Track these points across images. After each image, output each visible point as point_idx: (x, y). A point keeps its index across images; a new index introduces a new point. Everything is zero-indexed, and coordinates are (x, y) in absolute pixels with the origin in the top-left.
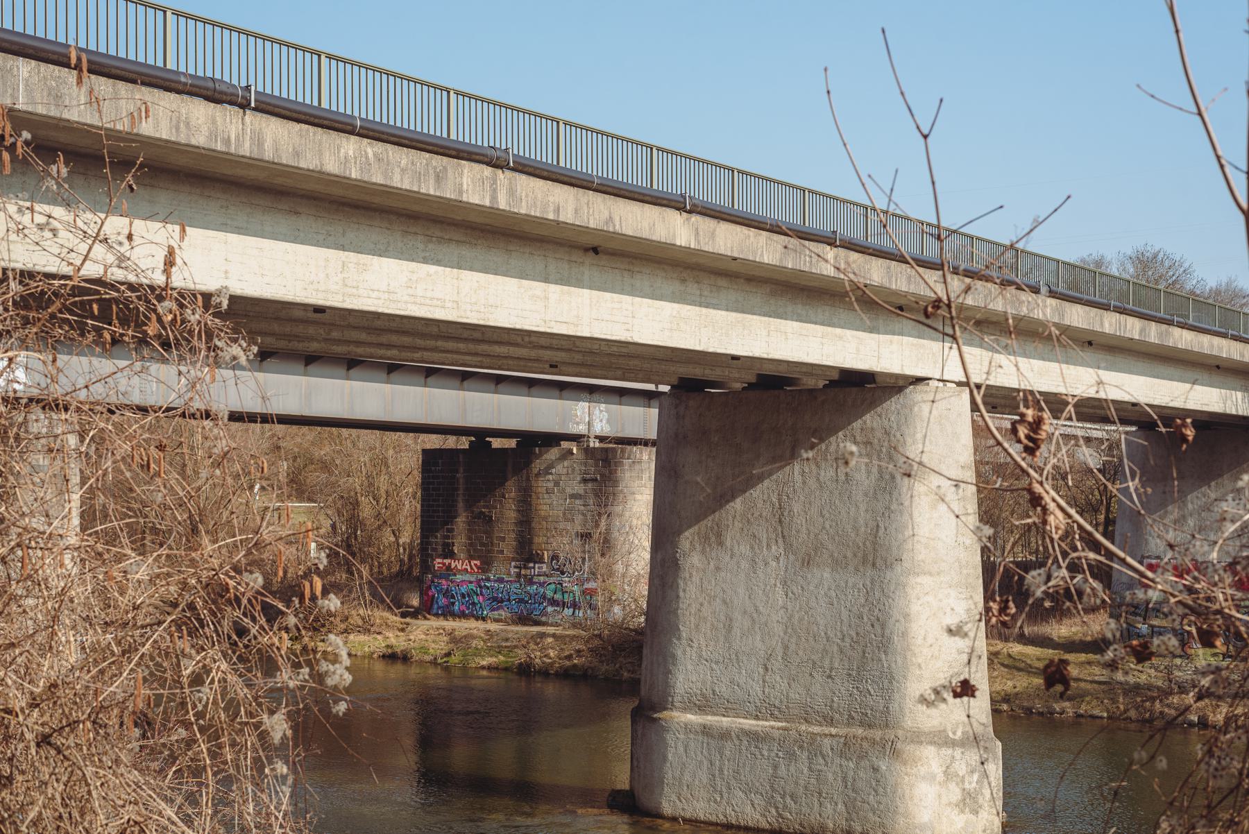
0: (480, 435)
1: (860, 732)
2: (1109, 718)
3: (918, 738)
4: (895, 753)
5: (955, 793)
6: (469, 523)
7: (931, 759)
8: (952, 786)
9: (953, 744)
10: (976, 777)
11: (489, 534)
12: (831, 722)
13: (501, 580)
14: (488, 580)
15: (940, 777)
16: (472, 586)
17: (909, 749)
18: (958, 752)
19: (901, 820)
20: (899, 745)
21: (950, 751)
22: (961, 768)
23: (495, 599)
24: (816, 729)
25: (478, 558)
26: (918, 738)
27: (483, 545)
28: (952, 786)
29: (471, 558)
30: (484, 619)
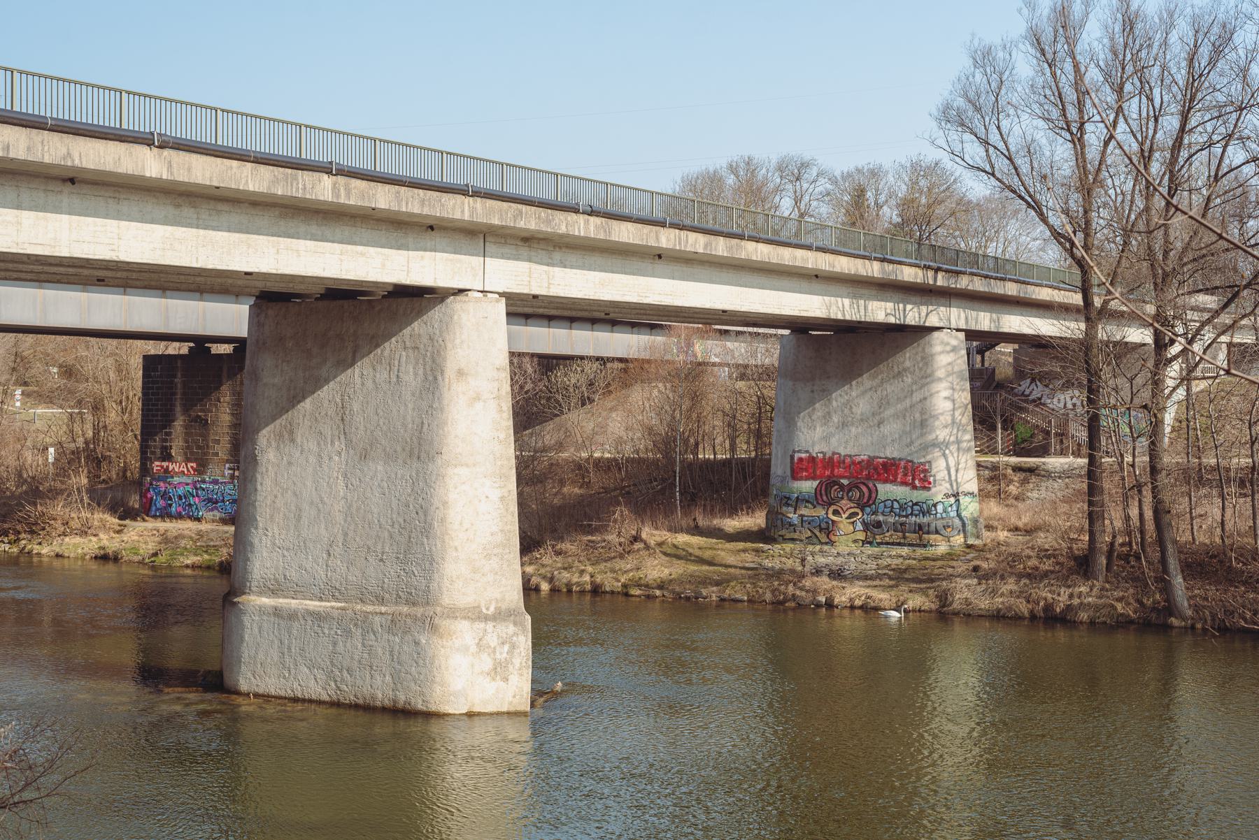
0: (200, 342)
1: (405, 609)
2: (749, 601)
3: (453, 613)
4: (434, 628)
5: (487, 663)
6: (186, 427)
7: (464, 633)
8: (485, 656)
9: (486, 618)
10: (506, 648)
11: (205, 437)
12: (382, 601)
13: (215, 482)
14: (204, 481)
15: (473, 649)
16: (188, 488)
17: (444, 624)
18: (490, 625)
19: (438, 689)
20: (437, 621)
21: (482, 625)
22: (492, 640)
23: (210, 500)
24: (369, 608)
25: (195, 461)
26: (453, 613)
27: (199, 447)
28: (485, 656)
29: (187, 460)
30: (198, 520)
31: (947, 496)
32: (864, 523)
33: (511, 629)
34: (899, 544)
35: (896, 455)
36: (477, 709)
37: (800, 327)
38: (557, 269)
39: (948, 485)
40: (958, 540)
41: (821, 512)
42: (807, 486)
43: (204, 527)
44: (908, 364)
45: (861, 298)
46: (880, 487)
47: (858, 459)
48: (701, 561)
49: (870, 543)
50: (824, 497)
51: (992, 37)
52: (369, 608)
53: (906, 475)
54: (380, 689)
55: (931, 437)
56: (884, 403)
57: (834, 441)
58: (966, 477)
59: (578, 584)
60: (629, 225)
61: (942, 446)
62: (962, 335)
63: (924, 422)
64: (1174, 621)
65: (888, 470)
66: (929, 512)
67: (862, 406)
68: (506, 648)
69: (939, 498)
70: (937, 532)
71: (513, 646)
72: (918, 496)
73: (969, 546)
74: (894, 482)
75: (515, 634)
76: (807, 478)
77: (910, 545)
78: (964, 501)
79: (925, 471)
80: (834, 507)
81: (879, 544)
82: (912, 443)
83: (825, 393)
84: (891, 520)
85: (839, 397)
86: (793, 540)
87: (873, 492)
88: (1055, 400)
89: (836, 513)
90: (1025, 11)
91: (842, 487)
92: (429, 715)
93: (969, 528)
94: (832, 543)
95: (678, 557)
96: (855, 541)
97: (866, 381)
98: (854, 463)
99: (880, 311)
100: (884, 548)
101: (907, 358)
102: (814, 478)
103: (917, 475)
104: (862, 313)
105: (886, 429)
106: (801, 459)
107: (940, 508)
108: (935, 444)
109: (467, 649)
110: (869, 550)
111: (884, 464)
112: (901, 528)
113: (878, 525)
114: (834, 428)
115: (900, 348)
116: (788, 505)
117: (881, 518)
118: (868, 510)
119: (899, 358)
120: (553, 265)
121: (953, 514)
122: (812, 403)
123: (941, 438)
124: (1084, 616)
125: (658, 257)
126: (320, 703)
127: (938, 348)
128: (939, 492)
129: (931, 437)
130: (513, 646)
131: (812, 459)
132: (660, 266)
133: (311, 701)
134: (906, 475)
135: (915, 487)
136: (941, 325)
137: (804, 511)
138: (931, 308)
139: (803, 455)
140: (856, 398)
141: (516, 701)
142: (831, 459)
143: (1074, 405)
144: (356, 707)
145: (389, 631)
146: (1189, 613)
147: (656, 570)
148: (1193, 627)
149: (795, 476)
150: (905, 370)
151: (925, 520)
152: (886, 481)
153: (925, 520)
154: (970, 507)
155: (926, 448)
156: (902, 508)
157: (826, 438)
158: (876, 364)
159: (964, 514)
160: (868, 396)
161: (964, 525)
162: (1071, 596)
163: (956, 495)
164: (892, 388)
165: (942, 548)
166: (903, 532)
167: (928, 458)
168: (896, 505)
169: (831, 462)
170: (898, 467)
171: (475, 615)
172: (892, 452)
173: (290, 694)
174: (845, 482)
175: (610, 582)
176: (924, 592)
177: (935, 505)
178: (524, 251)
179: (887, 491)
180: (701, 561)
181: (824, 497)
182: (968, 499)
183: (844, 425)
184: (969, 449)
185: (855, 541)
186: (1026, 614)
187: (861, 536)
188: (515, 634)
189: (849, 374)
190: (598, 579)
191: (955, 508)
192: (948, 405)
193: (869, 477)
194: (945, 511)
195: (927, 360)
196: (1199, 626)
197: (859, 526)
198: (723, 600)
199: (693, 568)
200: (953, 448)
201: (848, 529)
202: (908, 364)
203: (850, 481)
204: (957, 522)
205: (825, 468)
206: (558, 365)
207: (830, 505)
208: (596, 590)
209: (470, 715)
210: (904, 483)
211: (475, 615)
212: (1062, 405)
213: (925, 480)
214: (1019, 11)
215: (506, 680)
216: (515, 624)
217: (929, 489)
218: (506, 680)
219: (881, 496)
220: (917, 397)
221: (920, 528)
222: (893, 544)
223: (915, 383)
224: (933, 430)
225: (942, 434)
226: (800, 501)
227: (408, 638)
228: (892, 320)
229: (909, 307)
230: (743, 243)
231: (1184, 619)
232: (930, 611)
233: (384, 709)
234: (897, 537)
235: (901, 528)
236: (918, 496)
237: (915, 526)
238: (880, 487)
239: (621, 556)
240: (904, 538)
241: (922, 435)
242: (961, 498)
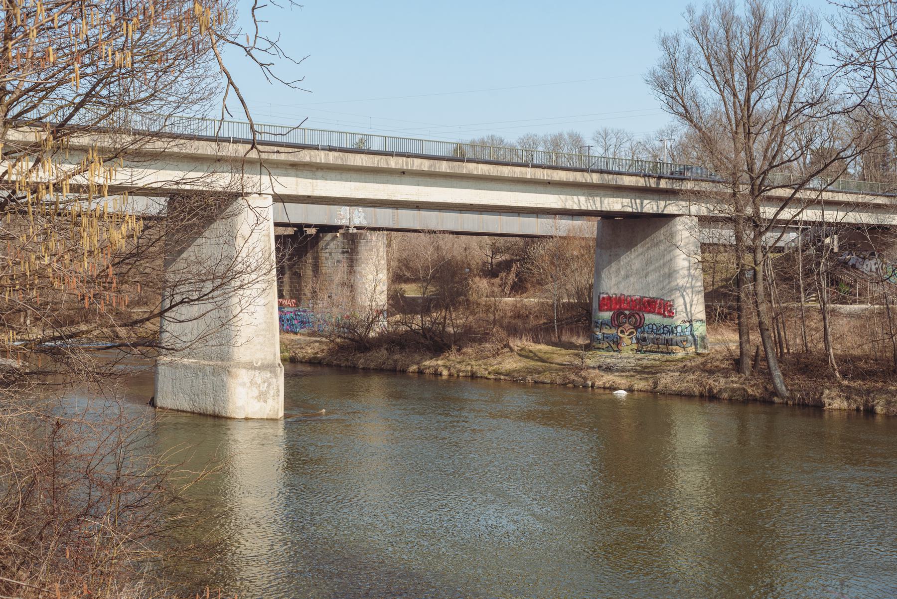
0: (300, 227)
1: (219, 363)
2: (551, 383)
3: (239, 365)
4: (229, 373)
5: (255, 392)
6: (291, 278)
7: (243, 375)
8: (254, 389)
9: (255, 368)
10: (266, 384)
11: (300, 284)
12: (211, 359)
13: (305, 311)
14: (299, 311)
15: (248, 384)
16: (292, 315)
17: (234, 370)
18: (257, 372)
19: (231, 405)
20: (230, 369)
21: (253, 372)
22: (259, 380)
23: (302, 322)
24: (206, 362)
25: (295, 298)
26: (239, 365)
27: (297, 290)
28: (254, 389)
29: (291, 298)
30: (296, 334)
31: (684, 322)
32: (637, 339)
33: (269, 375)
34: (656, 352)
35: (655, 295)
36: (250, 416)
37: (607, 217)
38: (319, 181)
39: (685, 315)
40: (692, 349)
41: (613, 331)
42: (607, 315)
43: (298, 337)
44: (662, 237)
45: (597, 195)
46: (646, 315)
47: (634, 298)
48: (542, 360)
49: (640, 351)
50: (615, 323)
51: (670, 32)
52: (206, 362)
53: (660, 308)
54: (209, 406)
55: (674, 284)
56: (648, 263)
57: (621, 286)
58: (697, 310)
59: (463, 371)
60: (363, 156)
61: (681, 289)
62: (696, 219)
63: (670, 275)
64: (776, 399)
65: (650, 305)
66: (673, 332)
67: (637, 264)
68: (266, 384)
69: (679, 323)
70: (677, 345)
71: (270, 384)
72: (666, 321)
73: (698, 354)
74: (653, 312)
75: (271, 377)
76: (607, 310)
77: (662, 353)
78: (696, 325)
79: (671, 306)
80: (621, 328)
81: (645, 352)
82: (664, 288)
83: (617, 257)
84: (651, 337)
85: (624, 259)
86: (599, 348)
87: (642, 319)
88: (865, 266)
89: (622, 332)
90: (687, 14)
91: (625, 315)
92: (230, 418)
93: (699, 342)
94: (619, 351)
95: (527, 357)
96: (632, 350)
97: (639, 249)
98: (632, 300)
99: (650, 206)
100: (647, 354)
101: (661, 234)
102: (610, 310)
103: (665, 308)
104: (639, 206)
105: (650, 278)
106: (604, 298)
107: (679, 329)
108: (678, 288)
109: (245, 384)
110: (639, 355)
111: (648, 301)
112: (656, 342)
113: (644, 339)
114: (622, 279)
115: (657, 228)
116: (597, 327)
117: (646, 335)
118: (639, 330)
119: (657, 234)
120: (316, 179)
121: (688, 333)
122: (610, 263)
123: (681, 284)
124: (725, 395)
125: (402, 174)
126: (187, 412)
127: (680, 227)
128: (679, 319)
129: (674, 284)
130: (270, 384)
131: (610, 298)
132: (405, 178)
133: (183, 411)
134: (660, 308)
135: (665, 316)
136: (681, 212)
137: (605, 331)
138: (668, 202)
139: (605, 296)
140: (633, 259)
141: (271, 413)
142: (620, 298)
143: (877, 269)
144: (200, 414)
145: (212, 374)
146: (787, 394)
147: (510, 363)
148: (787, 403)
149: (601, 310)
150: (660, 241)
151: (670, 337)
152: (649, 312)
153: (670, 337)
154: (700, 329)
155: (672, 291)
156: (658, 329)
157: (617, 284)
158: (645, 238)
159: (695, 333)
160: (640, 258)
161: (695, 340)
162: (726, 383)
163: (690, 321)
164: (653, 252)
165: (681, 354)
166: (658, 344)
167: (673, 297)
168: (655, 327)
169: (620, 300)
170: (656, 302)
171: (250, 366)
172: (652, 294)
173: (176, 408)
174: (627, 312)
175: (481, 371)
176: (647, 379)
177: (676, 328)
178: (293, 172)
179: (651, 318)
180: (542, 360)
181: (615, 323)
182: (698, 324)
183: (627, 277)
184: (699, 292)
185: (632, 350)
186: (697, 394)
187: (635, 347)
188: (271, 377)
189: (630, 245)
190: (475, 368)
191: (689, 329)
192: (686, 264)
193: (640, 310)
194: (682, 331)
195: (672, 235)
196: (790, 402)
197: (634, 341)
198: (536, 382)
199: (532, 364)
200: (689, 291)
201: (628, 342)
202: (662, 237)
203: (631, 311)
204: (690, 338)
205: (616, 304)
206: (533, 242)
207: (619, 327)
208: (473, 376)
209: (246, 419)
210: (659, 314)
211: (250, 366)
212: (868, 269)
213: (670, 311)
214: (683, 15)
215: (265, 401)
216: (271, 372)
217: (672, 317)
218: (265, 401)
219: (647, 322)
220: (667, 258)
221: (667, 342)
222: (652, 352)
223: (665, 250)
224: (676, 279)
225: (681, 282)
226: (604, 324)
227: (219, 378)
228: (629, 210)
229: (646, 202)
230: (464, 164)
231: (783, 398)
232: (647, 391)
233: (210, 415)
234: (654, 347)
235: (656, 342)
236: (666, 321)
237: (664, 341)
238: (646, 315)
239: (494, 356)
240: (659, 348)
241: (669, 283)
242: (694, 324)
